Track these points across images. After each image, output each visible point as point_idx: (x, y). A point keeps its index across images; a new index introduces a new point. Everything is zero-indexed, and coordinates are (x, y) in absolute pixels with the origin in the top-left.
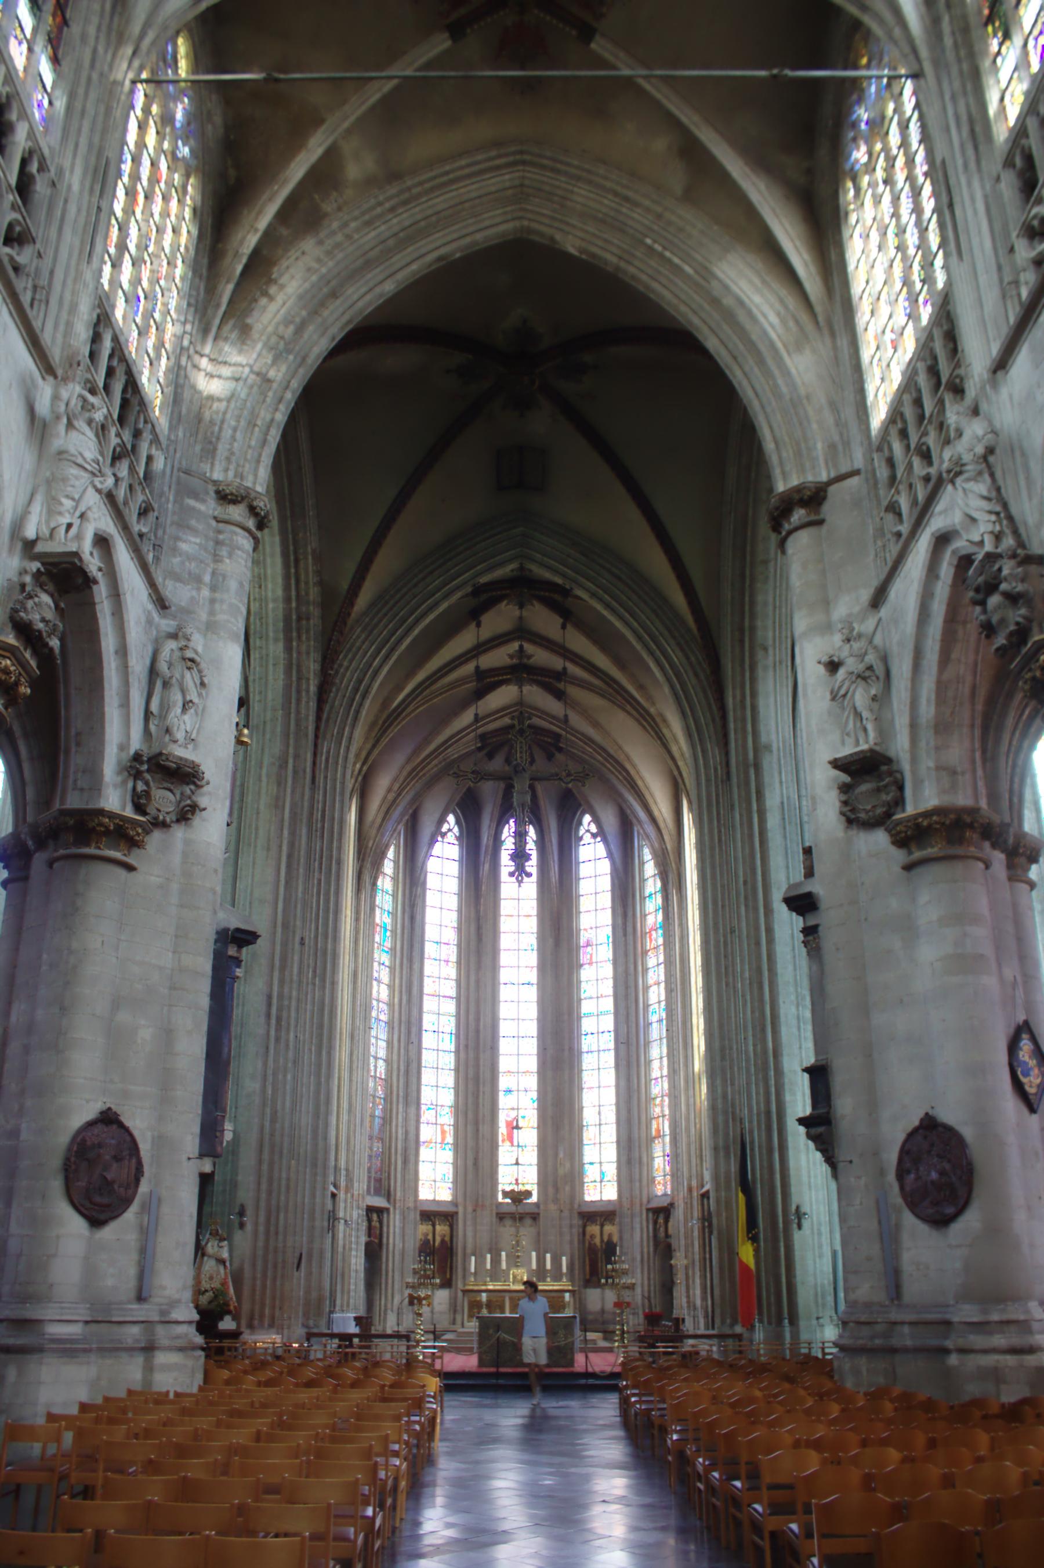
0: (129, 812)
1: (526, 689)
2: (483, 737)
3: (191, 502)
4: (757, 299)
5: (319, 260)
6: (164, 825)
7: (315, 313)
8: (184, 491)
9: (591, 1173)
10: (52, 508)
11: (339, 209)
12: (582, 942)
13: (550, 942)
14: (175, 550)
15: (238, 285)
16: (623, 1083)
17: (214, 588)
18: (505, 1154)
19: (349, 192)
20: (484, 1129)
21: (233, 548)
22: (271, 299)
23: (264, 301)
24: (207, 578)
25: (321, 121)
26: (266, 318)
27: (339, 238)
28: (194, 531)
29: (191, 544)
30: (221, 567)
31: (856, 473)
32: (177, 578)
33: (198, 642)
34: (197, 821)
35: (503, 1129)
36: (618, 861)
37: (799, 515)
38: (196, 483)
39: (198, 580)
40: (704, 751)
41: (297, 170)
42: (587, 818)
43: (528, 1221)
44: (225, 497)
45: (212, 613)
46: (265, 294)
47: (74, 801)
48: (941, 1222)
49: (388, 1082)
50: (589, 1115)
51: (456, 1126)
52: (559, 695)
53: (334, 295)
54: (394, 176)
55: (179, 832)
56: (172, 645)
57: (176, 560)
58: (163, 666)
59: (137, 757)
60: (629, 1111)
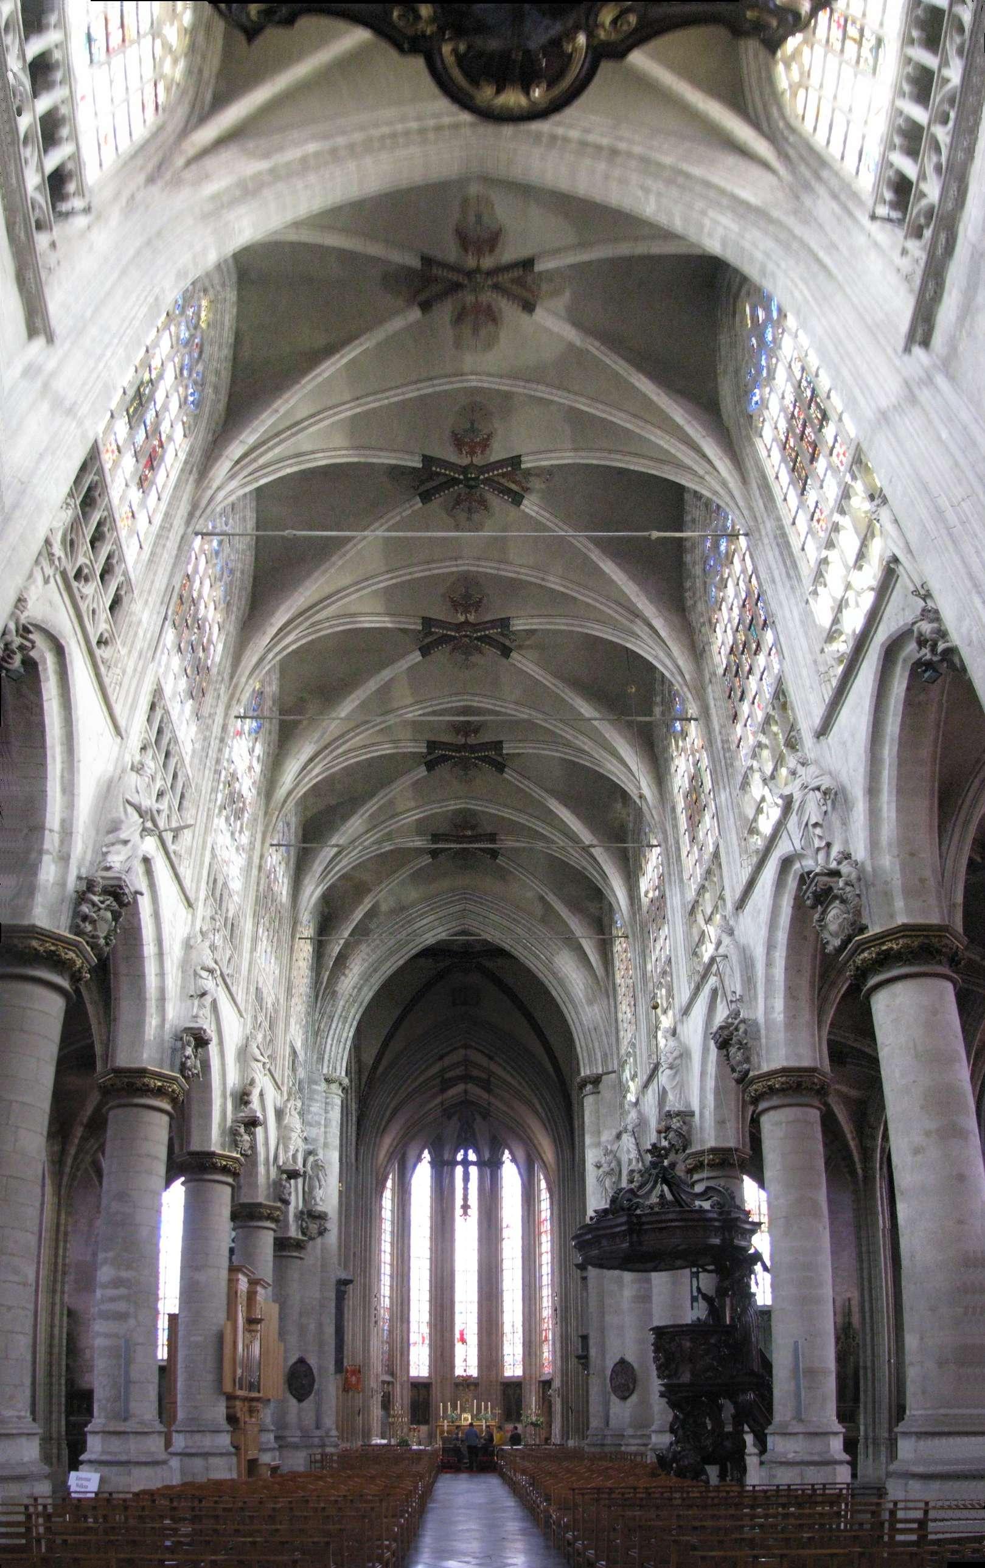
1: (470, 1086)
2: (445, 1110)
3: (315, 1087)
4: (574, 976)
5: (368, 954)
8: (312, 1082)
9: (508, 1360)
11: (378, 927)
12: (504, 1225)
13: (485, 1225)
14: (309, 1112)
15: (332, 971)
16: (527, 1310)
17: (326, 1126)
18: (459, 1348)
19: (382, 918)
20: (447, 1335)
22: (346, 976)
23: (343, 978)
24: (323, 1122)
25: (369, 891)
26: (345, 985)
27: (378, 942)
28: (317, 1101)
29: (316, 1107)
30: (329, 1115)
31: (614, 1072)
32: (310, 1125)
35: (457, 1336)
36: (525, 1177)
37: (589, 1087)
38: (316, 1076)
39: (319, 1124)
40: (562, 1151)
41: (358, 914)
42: (507, 1152)
43: (472, 1388)
44: (328, 1081)
45: (326, 1138)
46: (344, 974)
48: (624, 1398)
50: (507, 1328)
51: (430, 1335)
52: (489, 1091)
53: (375, 971)
54: (403, 909)
57: (310, 1117)
60: (530, 1325)
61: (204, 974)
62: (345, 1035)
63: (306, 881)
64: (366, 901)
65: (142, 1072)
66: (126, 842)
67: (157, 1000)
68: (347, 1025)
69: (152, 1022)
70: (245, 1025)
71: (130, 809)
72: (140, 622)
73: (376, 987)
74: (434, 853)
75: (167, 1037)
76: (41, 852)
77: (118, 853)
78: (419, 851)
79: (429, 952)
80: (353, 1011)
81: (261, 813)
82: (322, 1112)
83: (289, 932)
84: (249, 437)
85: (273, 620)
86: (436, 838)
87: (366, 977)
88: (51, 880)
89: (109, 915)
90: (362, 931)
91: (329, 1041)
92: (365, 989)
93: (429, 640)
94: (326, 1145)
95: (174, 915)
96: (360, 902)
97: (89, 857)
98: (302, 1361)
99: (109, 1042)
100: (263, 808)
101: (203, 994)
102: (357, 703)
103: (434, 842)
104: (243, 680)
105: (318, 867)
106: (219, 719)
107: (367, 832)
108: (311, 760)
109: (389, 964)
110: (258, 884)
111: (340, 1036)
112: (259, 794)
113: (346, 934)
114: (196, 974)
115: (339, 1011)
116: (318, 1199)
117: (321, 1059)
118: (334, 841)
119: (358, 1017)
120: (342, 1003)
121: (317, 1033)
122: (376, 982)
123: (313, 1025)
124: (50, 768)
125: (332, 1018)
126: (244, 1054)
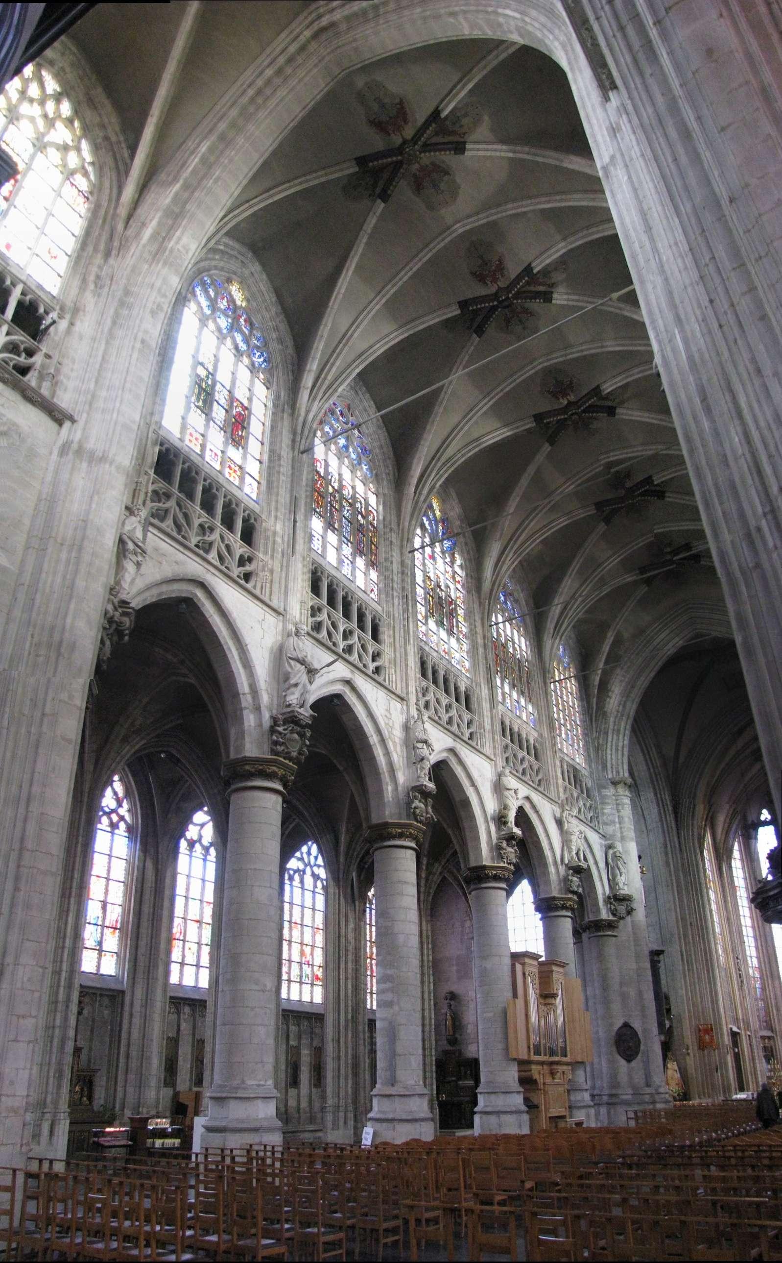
0: (611, 918)
6: (623, 918)
7: (628, 696)
8: (601, 787)
10: (570, 852)
14: (603, 814)
15: (598, 698)
21: (623, 804)
25: (609, 627)
29: (608, 810)
32: (605, 824)
33: (619, 846)
34: (634, 913)
41: (606, 648)
44: (615, 783)
47: (592, 918)
49: (760, 968)
53: (633, 687)
55: (629, 919)
56: (611, 852)
58: (610, 860)
59: (609, 898)
61: (420, 745)
62: (621, 744)
63: (545, 638)
64: (609, 634)
65: (386, 825)
66: (296, 685)
67: (389, 772)
68: (621, 736)
69: (389, 789)
70: (496, 765)
71: (292, 662)
72: (275, 533)
73: (638, 700)
74: (648, 582)
75: (401, 796)
76: (241, 710)
77: (293, 693)
78: (635, 583)
79: (673, 662)
80: (623, 724)
81: (476, 606)
82: (615, 812)
83: (541, 681)
84: (313, 365)
85: (412, 472)
86: (643, 570)
87: (626, 694)
88: (253, 725)
89: (296, 736)
90: (613, 659)
91: (609, 752)
92: (629, 704)
93: (550, 432)
94: (623, 838)
95: (388, 710)
96: (605, 637)
97: (275, 702)
98: (626, 1025)
99: (367, 810)
100: (476, 600)
101: (422, 759)
102: (518, 499)
103: (642, 573)
104: (407, 524)
105: (550, 626)
106: (396, 559)
107: (581, 586)
108: (503, 553)
109: (642, 679)
110: (486, 658)
111: (617, 746)
112: (468, 592)
113: (601, 665)
114: (414, 747)
115: (611, 727)
116: (621, 885)
117: (605, 767)
118: (556, 601)
119: (628, 727)
120: (612, 720)
121: (597, 749)
122: (637, 694)
123: (593, 742)
124: (229, 656)
125: (607, 733)
126: (499, 788)
